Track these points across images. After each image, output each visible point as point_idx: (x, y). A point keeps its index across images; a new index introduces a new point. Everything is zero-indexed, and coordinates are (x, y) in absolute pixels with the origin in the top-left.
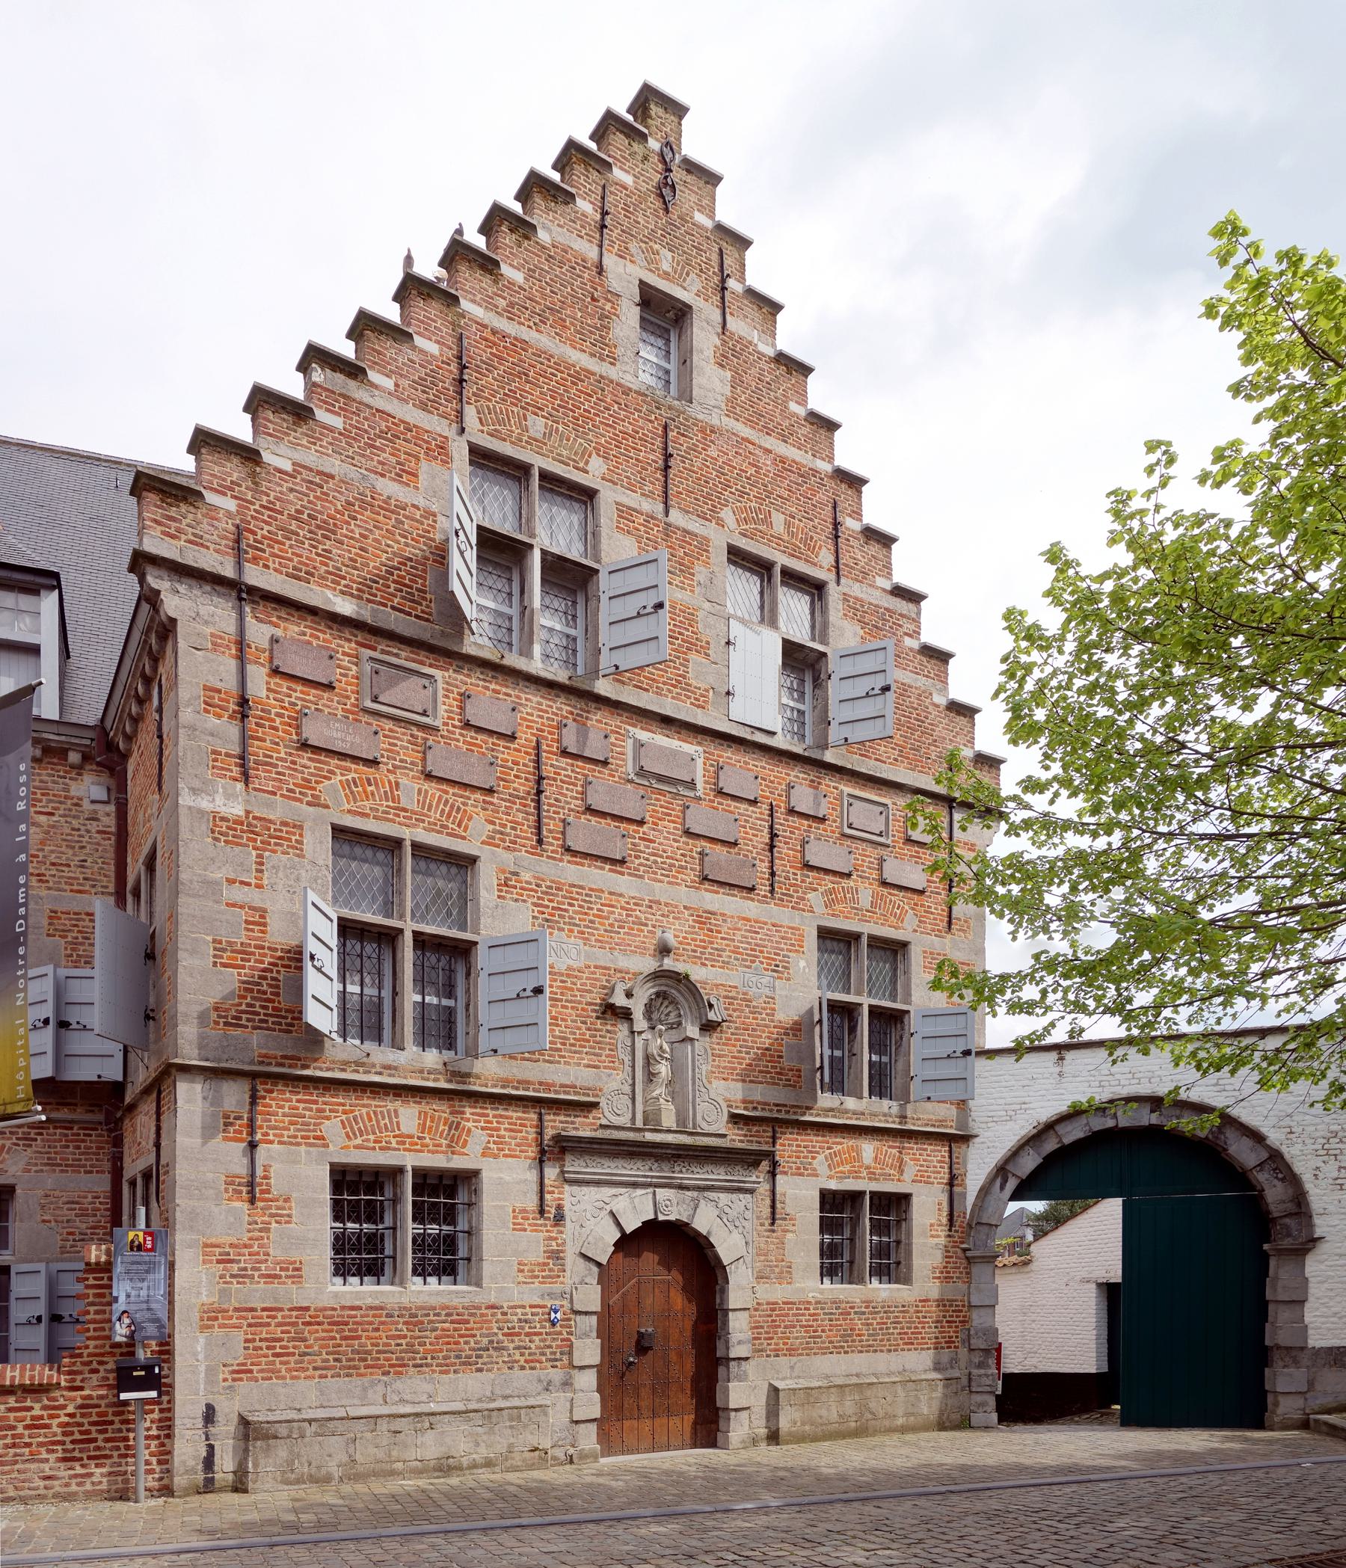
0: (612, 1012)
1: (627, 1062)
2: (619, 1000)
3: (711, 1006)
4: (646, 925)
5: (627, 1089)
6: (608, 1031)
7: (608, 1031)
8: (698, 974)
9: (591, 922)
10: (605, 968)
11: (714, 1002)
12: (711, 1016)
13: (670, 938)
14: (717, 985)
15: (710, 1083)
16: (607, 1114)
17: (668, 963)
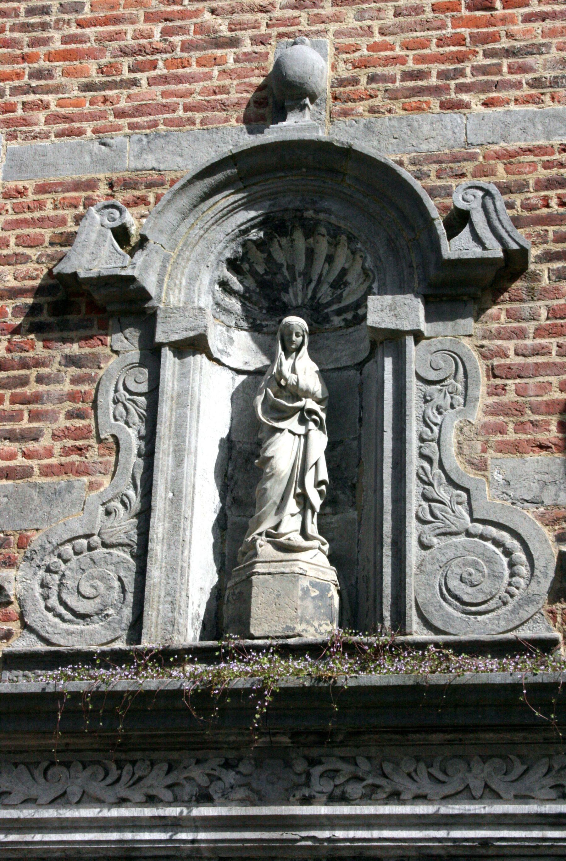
0: (78, 307)
1: (132, 439)
2: (95, 257)
3: (458, 220)
4: (233, 43)
5: (124, 525)
6: (71, 361)
7: (71, 361)
8: (394, 139)
9: (38, 74)
10: (77, 186)
11: (473, 205)
12: (458, 247)
13: (315, 62)
14: (508, 157)
15: (481, 466)
16: (39, 616)
17: (296, 126)
